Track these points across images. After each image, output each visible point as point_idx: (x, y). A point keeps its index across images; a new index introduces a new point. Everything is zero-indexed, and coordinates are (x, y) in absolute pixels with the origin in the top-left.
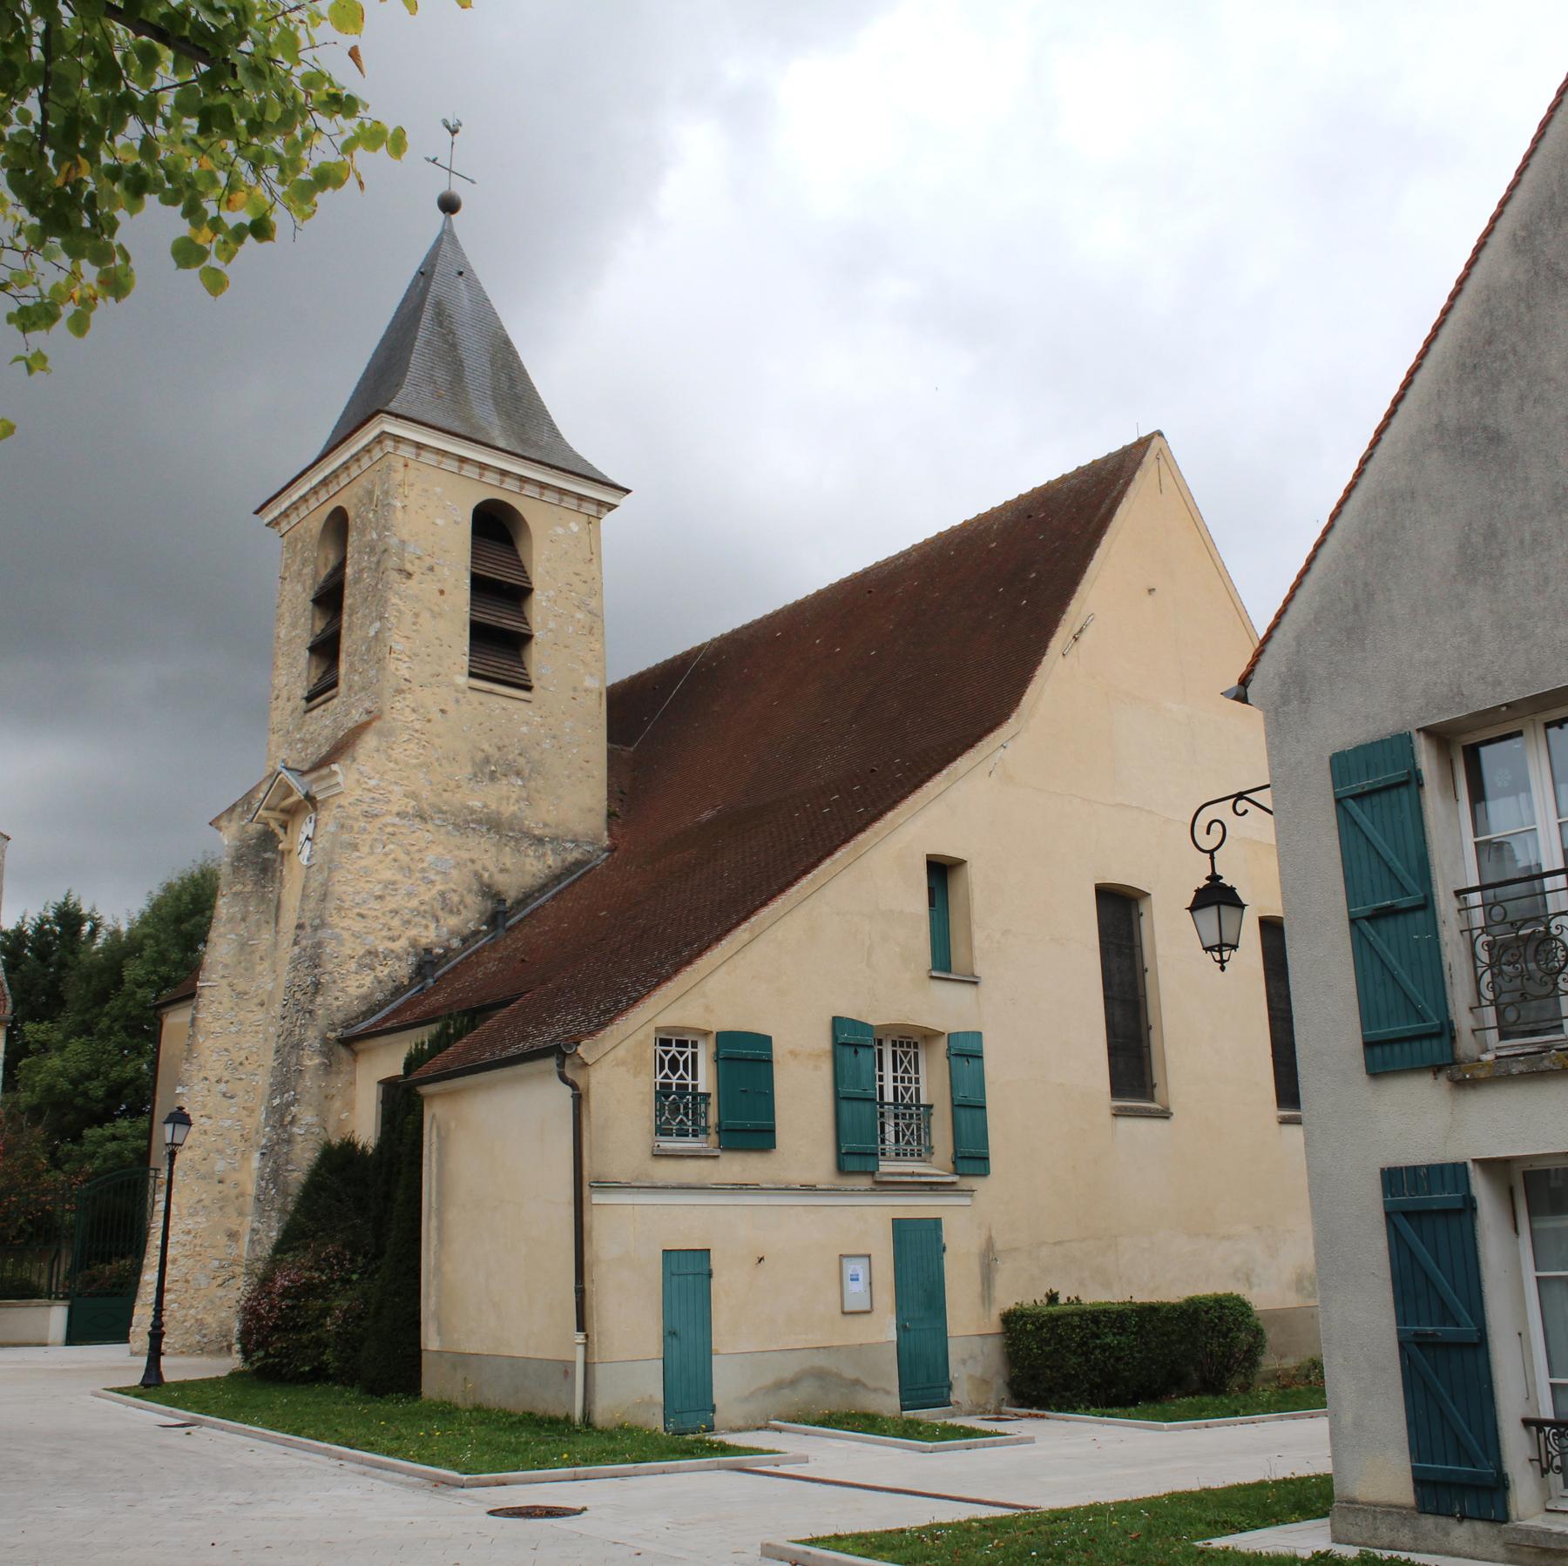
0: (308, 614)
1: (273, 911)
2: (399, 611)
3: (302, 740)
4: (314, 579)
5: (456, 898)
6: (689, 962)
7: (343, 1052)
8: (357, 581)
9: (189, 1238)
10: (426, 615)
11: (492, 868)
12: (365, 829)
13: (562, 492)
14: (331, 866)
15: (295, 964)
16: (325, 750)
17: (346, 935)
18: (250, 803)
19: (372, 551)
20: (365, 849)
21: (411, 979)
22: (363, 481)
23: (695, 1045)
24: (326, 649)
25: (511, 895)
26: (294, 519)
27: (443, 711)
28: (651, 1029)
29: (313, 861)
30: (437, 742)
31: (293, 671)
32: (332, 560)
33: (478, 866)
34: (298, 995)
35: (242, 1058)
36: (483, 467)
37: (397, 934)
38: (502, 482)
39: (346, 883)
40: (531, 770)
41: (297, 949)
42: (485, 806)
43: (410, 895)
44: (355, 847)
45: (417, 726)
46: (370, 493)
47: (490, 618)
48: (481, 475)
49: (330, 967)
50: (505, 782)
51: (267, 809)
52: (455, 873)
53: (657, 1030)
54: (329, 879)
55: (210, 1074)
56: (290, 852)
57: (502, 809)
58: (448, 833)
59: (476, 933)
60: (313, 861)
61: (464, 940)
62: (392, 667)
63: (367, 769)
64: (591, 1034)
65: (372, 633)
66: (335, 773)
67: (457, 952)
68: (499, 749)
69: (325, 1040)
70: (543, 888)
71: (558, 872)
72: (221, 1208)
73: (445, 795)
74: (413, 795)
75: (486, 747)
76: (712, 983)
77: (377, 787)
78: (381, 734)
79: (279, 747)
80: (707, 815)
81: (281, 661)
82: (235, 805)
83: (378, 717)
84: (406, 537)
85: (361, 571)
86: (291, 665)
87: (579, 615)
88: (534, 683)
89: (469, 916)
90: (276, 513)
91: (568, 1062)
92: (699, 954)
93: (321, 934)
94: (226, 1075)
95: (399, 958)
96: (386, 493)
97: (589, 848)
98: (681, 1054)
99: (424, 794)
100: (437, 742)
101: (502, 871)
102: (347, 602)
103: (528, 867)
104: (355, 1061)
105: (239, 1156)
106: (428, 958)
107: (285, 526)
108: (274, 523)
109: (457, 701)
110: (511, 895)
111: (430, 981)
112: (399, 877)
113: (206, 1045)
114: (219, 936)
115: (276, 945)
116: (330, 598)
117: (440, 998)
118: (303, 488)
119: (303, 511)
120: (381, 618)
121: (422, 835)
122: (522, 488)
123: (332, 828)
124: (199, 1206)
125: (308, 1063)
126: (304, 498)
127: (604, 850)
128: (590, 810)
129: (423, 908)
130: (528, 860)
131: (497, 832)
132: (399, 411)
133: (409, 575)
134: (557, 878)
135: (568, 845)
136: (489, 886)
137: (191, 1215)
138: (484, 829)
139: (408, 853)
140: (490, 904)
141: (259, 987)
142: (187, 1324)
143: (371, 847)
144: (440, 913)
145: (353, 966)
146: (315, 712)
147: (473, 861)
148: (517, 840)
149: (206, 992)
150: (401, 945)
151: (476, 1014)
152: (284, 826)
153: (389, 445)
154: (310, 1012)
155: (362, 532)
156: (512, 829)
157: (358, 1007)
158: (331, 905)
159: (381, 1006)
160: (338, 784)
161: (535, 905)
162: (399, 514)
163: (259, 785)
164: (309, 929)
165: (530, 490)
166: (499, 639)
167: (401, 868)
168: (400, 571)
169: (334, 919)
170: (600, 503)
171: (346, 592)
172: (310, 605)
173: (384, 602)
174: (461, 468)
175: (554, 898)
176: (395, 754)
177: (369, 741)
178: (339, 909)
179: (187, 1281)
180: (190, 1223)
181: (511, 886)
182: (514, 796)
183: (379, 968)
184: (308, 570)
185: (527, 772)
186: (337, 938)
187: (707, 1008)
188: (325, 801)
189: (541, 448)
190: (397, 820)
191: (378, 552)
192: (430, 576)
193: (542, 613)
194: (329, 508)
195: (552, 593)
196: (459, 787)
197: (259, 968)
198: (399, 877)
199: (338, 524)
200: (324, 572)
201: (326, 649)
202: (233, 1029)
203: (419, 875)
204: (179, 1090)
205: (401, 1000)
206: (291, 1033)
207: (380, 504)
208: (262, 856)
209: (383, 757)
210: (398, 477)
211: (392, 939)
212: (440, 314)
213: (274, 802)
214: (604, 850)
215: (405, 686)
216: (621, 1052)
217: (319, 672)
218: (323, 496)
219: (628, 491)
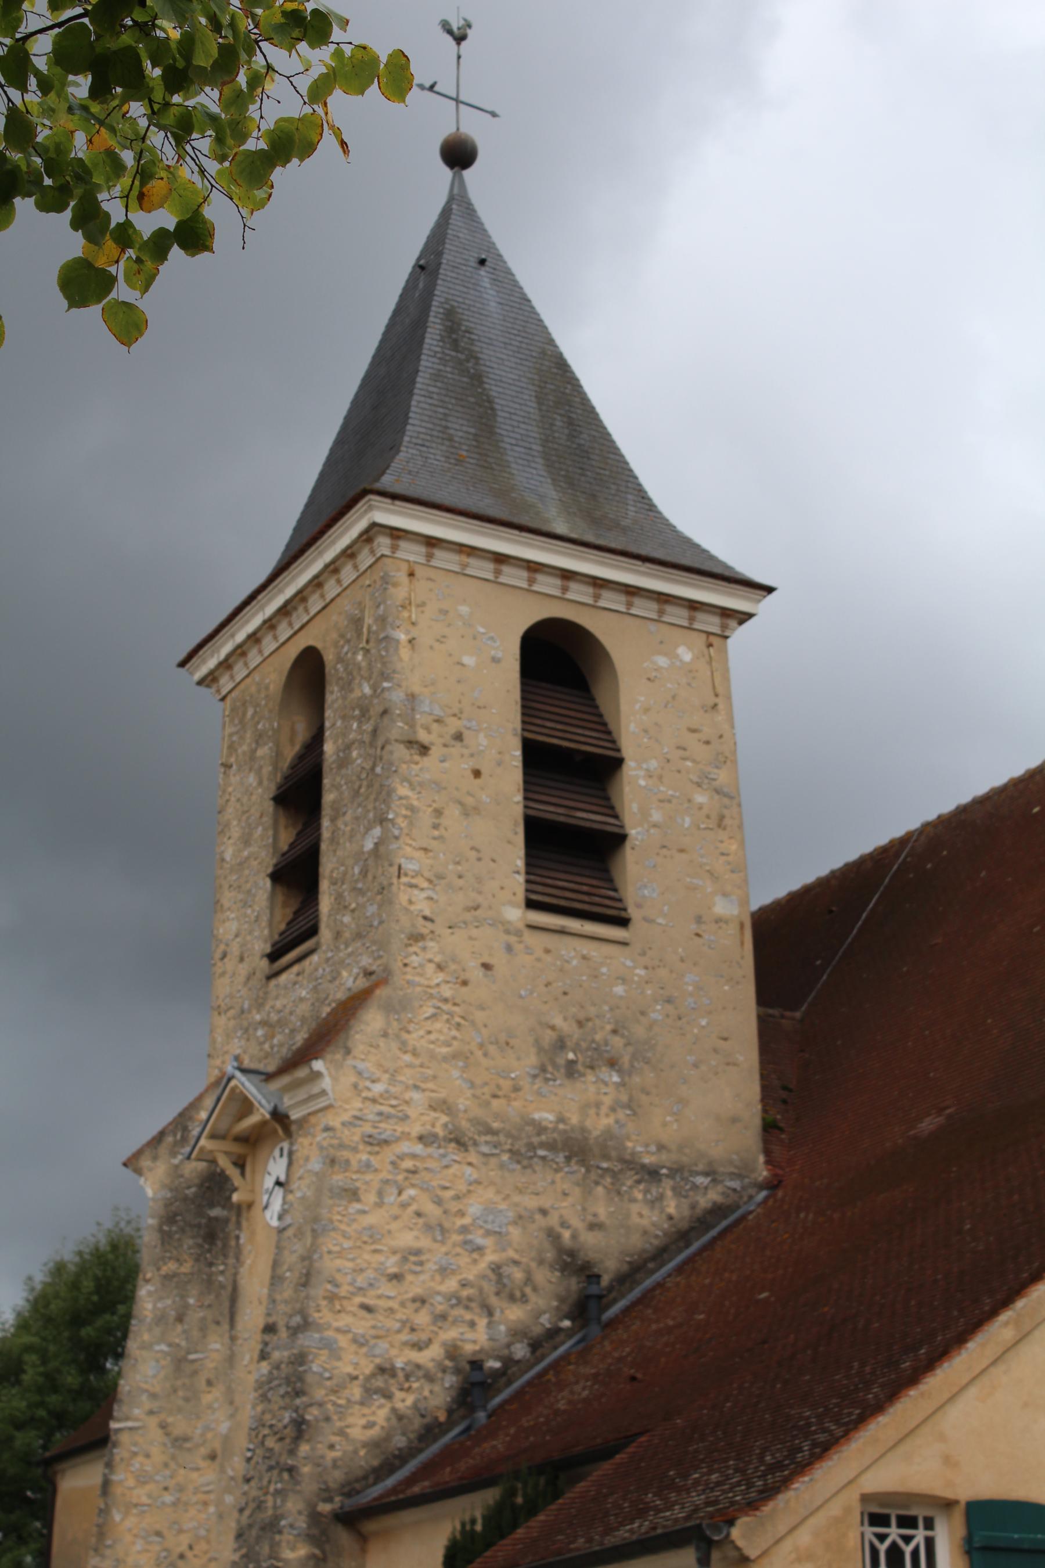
0: (267, 820)
1: (227, 1304)
2: (412, 808)
3: (264, 1023)
4: (276, 768)
5: (518, 1275)
6: (913, 1379)
7: (343, 1537)
8: (343, 762)
10: (453, 812)
11: (576, 1222)
12: (368, 1165)
13: (664, 599)
14: (315, 1226)
15: (264, 1390)
16: (300, 1038)
17: (343, 1341)
18: (185, 1129)
19: (365, 713)
20: (370, 1198)
21: (450, 1412)
22: (346, 605)
23: (929, 1524)
24: (298, 875)
25: (609, 1267)
26: (240, 671)
27: (486, 966)
28: (852, 1497)
29: (288, 1220)
30: (479, 1016)
31: (247, 915)
32: (302, 733)
33: (553, 1220)
34: (270, 1443)
35: (183, 1548)
36: (533, 568)
37: (424, 1337)
38: (565, 589)
39: (340, 1255)
40: (634, 1057)
41: (265, 1367)
42: (561, 1119)
43: (444, 1271)
44: (353, 1195)
45: (447, 992)
46: (357, 622)
47: (553, 811)
48: (531, 581)
49: (319, 1394)
50: (591, 1077)
51: (213, 1136)
52: (515, 1233)
53: (865, 1498)
54: (314, 1248)
56: (250, 1205)
57: (588, 1123)
58: (502, 1166)
59: (553, 1334)
60: (288, 1220)
61: (535, 1345)
62: (403, 898)
63: (368, 1066)
64: (752, 1506)
65: (369, 845)
66: (318, 1075)
67: (524, 1365)
68: (580, 1024)
69: (315, 1517)
70: (660, 1255)
71: (684, 1225)
73: (495, 1103)
74: (443, 1106)
75: (558, 1021)
76: (955, 1413)
77: (386, 1095)
78: (389, 1008)
79: (228, 1036)
80: (928, 1125)
81: (228, 898)
82: (162, 1134)
83: (383, 982)
84: (416, 689)
85: (348, 747)
86: (245, 904)
87: (700, 798)
88: (633, 912)
89: (540, 1305)
90: (212, 663)
91: (715, 1555)
92: (929, 1365)
93: (307, 1340)
95: (429, 1378)
96: (382, 620)
97: (735, 1184)
98: (907, 1539)
99: (462, 1103)
100: (479, 1016)
101: (593, 1226)
102: (328, 798)
103: (635, 1219)
104: (364, 1551)
106: (477, 1377)
107: (226, 683)
108: (209, 680)
109: (509, 948)
110: (609, 1267)
111: (481, 1416)
112: (425, 1242)
113: (125, 1524)
114: (144, 1347)
115: (231, 1359)
116: (300, 794)
117: (498, 1444)
118: (253, 622)
119: (254, 658)
120: (382, 820)
121: (461, 1170)
122: (597, 597)
123: (316, 1164)
125: (288, 1554)
126: (254, 638)
127: (761, 1187)
128: (734, 1120)
129: (465, 1293)
130: (635, 1208)
131: (582, 1162)
132: (398, 489)
133: (425, 750)
134: (682, 1237)
135: (700, 1180)
136: (572, 1253)
138: (561, 1158)
139: (439, 1202)
140: (574, 1284)
141: (207, 1428)
143: (380, 1194)
144: (494, 1301)
145: (356, 1392)
146: (283, 978)
147: (544, 1212)
148: (614, 1175)
149: (124, 1438)
150: (434, 1353)
151: (558, 1471)
152: (240, 1164)
153: (383, 544)
154: (291, 1470)
155: (347, 686)
156: (606, 1157)
157: (365, 1460)
158: (319, 1290)
159: (402, 1457)
160: (323, 1093)
161: (648, 1283)
162: (405, 653)
163: (200, 1098)
164: (283, 1333)
165: (611, 600)
166: (573, 850)
167: (428, 1228)
168: (410, 743)
169: (323, 1315)
170: (726, 613)
171: (326, 782)
172: (269, 806)
173: (385, 795)
174: (498, 573)
175: (679, 1270)
176: (414, 1038)
177: (371, 1021)
178: (332, 1298)
181: (608, 1251)
182: (607, 1101)
183: (399, 1395)
184: (264, 751)
185: (626, 1060)
186: (330, 1346)
187: (948, 1461)
188: (303, 1121)
189: (625, 530)
190: (419, 1148)
191: (376, 715)
192: (456, 749)
193: (643, 796)
194: (293, 651)
195: (653, 764)
196: (516, 1089)
197: (207, 1399)
198: (425, 1242)
199: (309, 674)
200: (290, 753)
201: (298, 875)
202: (168, 1498)
203: (456, 1238)
205: (435, 1448)
206: (260, 1506)
207: (372, 636)
208: (208, 1214)
209: (394, 1045)
210: (399, 593)
211: (418, 1346)
212: (454, 329)
213: (223, 1126)
214: (761, 1187)
215: (424, 928)
216: (804, 1537)
217: (289, 913)
218: (284, 631)
219: (770, 590)
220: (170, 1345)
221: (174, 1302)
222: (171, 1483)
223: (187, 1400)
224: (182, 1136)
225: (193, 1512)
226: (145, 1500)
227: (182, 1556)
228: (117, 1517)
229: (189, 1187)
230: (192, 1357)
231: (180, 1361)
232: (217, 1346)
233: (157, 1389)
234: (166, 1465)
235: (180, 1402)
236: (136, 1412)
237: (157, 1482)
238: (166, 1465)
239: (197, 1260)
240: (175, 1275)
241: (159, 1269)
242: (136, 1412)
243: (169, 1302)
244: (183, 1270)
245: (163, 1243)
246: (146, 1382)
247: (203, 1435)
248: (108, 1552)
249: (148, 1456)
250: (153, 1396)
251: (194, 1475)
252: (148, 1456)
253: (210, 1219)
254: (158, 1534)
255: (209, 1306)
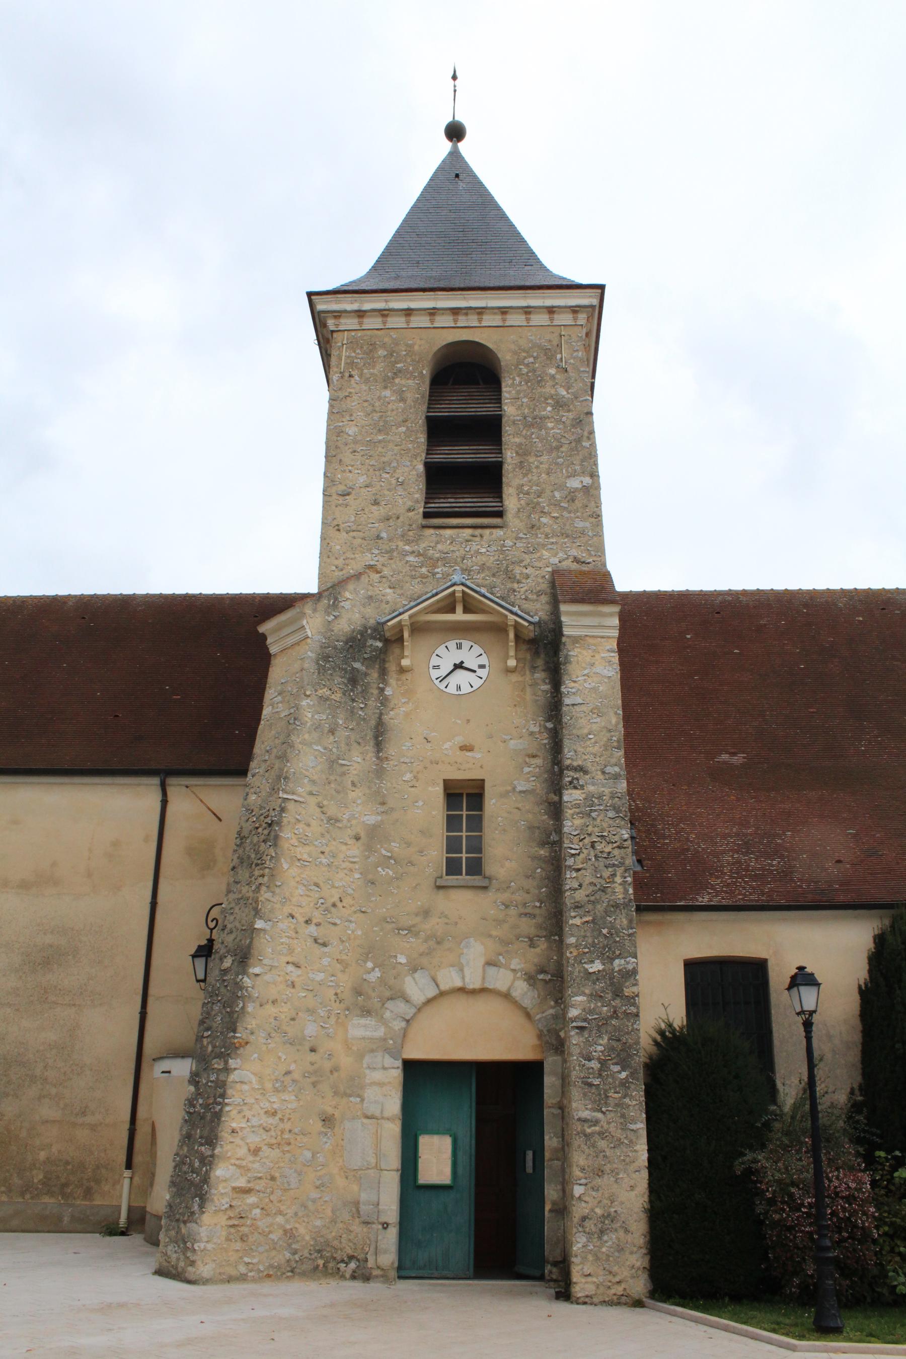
9: (271, 1121)
35: (335, 899)
55: (297, 912)
72: (314, 1084)
94: (317, 916)
105: (333, 1020)
124: (287, 1079)
137: (276, 1090)
141: (353, 817)
142: (271, 1236)
179: (273, 1179)
180: (275, 1101)
204: (259, 924)
220: (325, 748)
221: (327, 718)
222: (327, 850)
223: (338, 792)
224: (334, 603)
225: (341, 875)
226: (305, 857)
227: (334, 905)
228: (285, 866)
229: (337, 641)
230: (340, 761)
231: (333, 762)
232: (359, 760)
233: (315, 777)
234: (322, 835)
235: (334, 793)
236: (300, 790)
237: (316, 846)
238: (322, 835)
239: (344, 695)
240: (327, 699)
241: (316, 691)
242: (300, 790)
243: (324, 717)
244: (333, 697)
245: (319, 673)
246: (307, 770)
247: (349, 821)
248: (277, 890)
249: (309, 825)
250: (313, 782)
251: (344, 848)
252: (309, 825)
253: (353, 669)
254: (317, 885)
255: (352, 729)
